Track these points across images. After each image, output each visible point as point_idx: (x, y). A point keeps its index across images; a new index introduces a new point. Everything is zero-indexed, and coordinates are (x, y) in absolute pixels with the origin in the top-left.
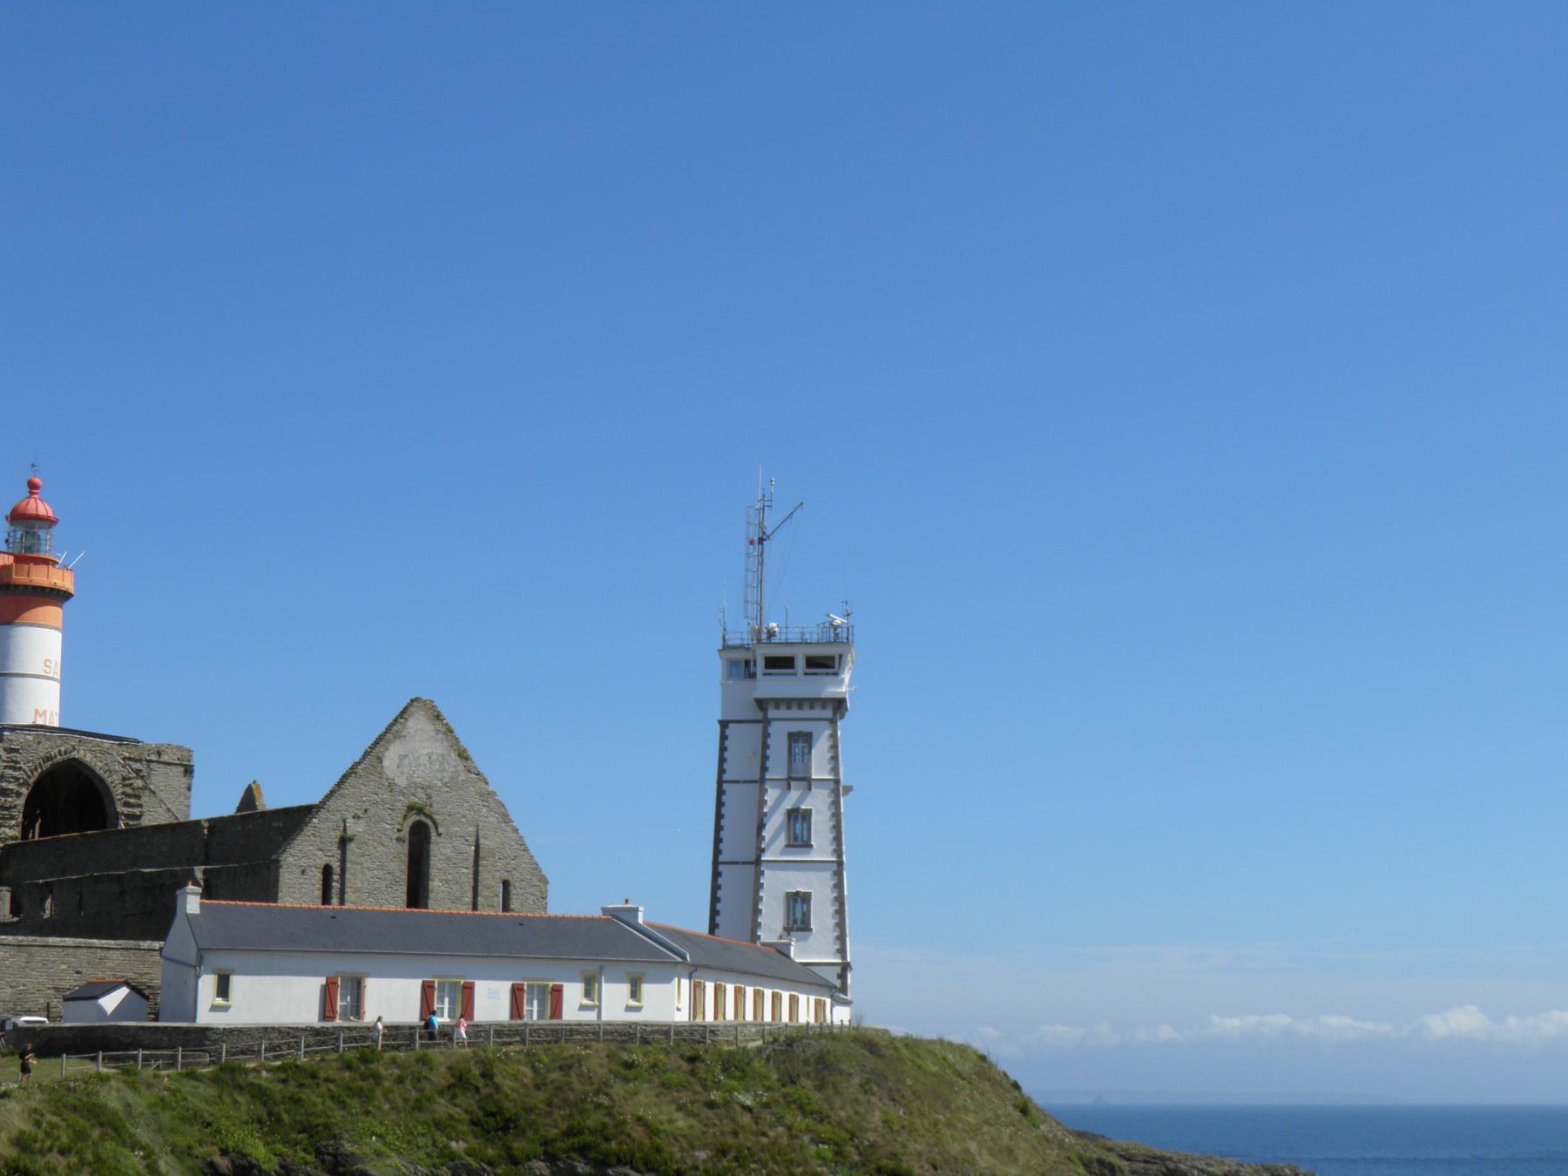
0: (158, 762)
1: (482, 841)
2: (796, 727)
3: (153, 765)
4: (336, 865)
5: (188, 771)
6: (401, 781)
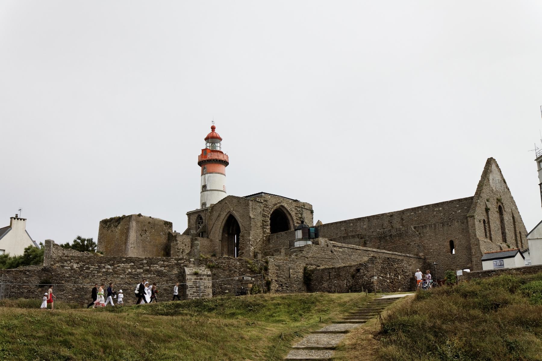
0: (304, 208)
1: (514, 215)
3: (303, 209)
4: (486, 220)
5: (312, 212)
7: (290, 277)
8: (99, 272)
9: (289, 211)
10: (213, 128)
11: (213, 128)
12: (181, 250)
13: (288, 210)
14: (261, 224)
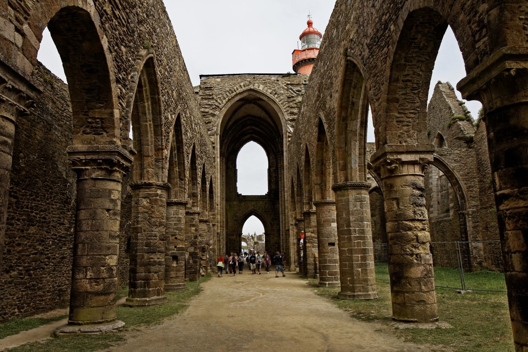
9: (271, 96)
10: (310, 24)
11: (310, 24)
13: (268, 94)
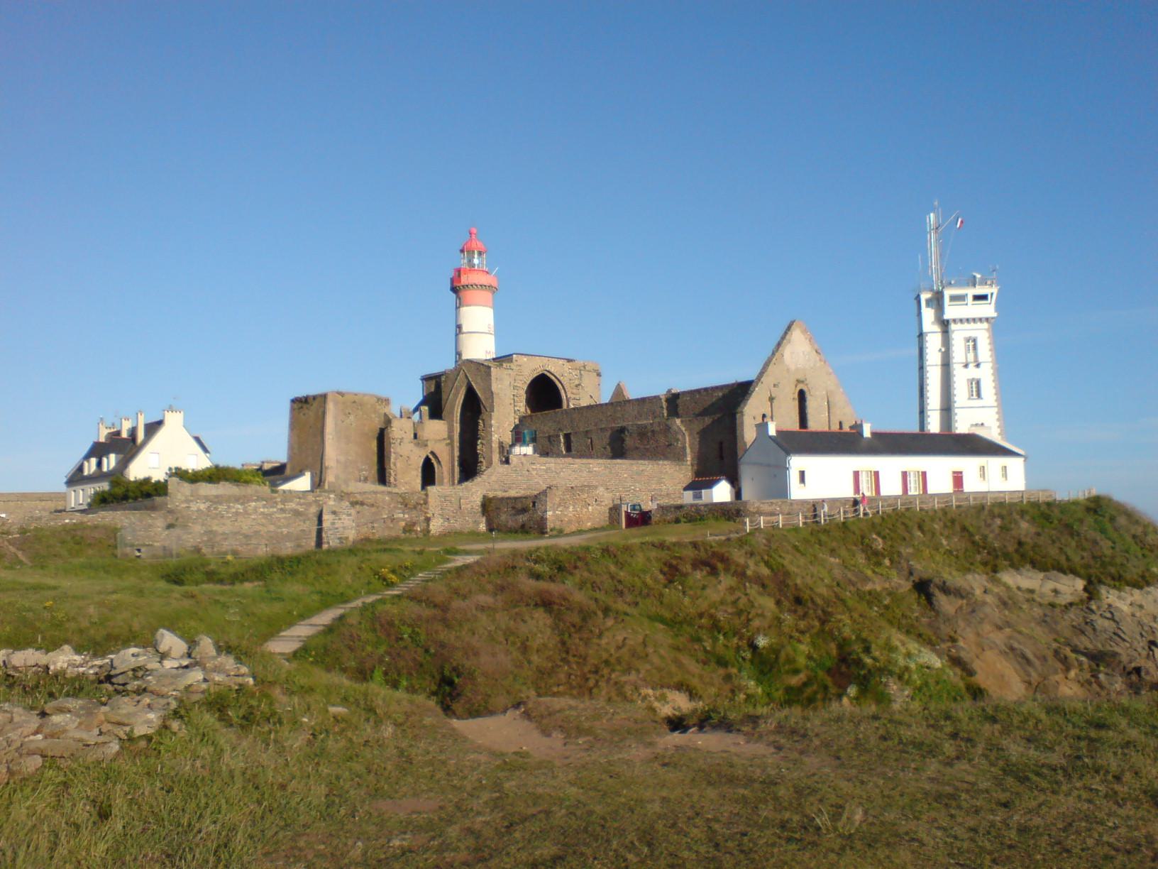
2: (968, 334)
6: (793, 367)
7: (460, 508)
8: (228, 512)
12: (399, 441)
14: (512, 402)
